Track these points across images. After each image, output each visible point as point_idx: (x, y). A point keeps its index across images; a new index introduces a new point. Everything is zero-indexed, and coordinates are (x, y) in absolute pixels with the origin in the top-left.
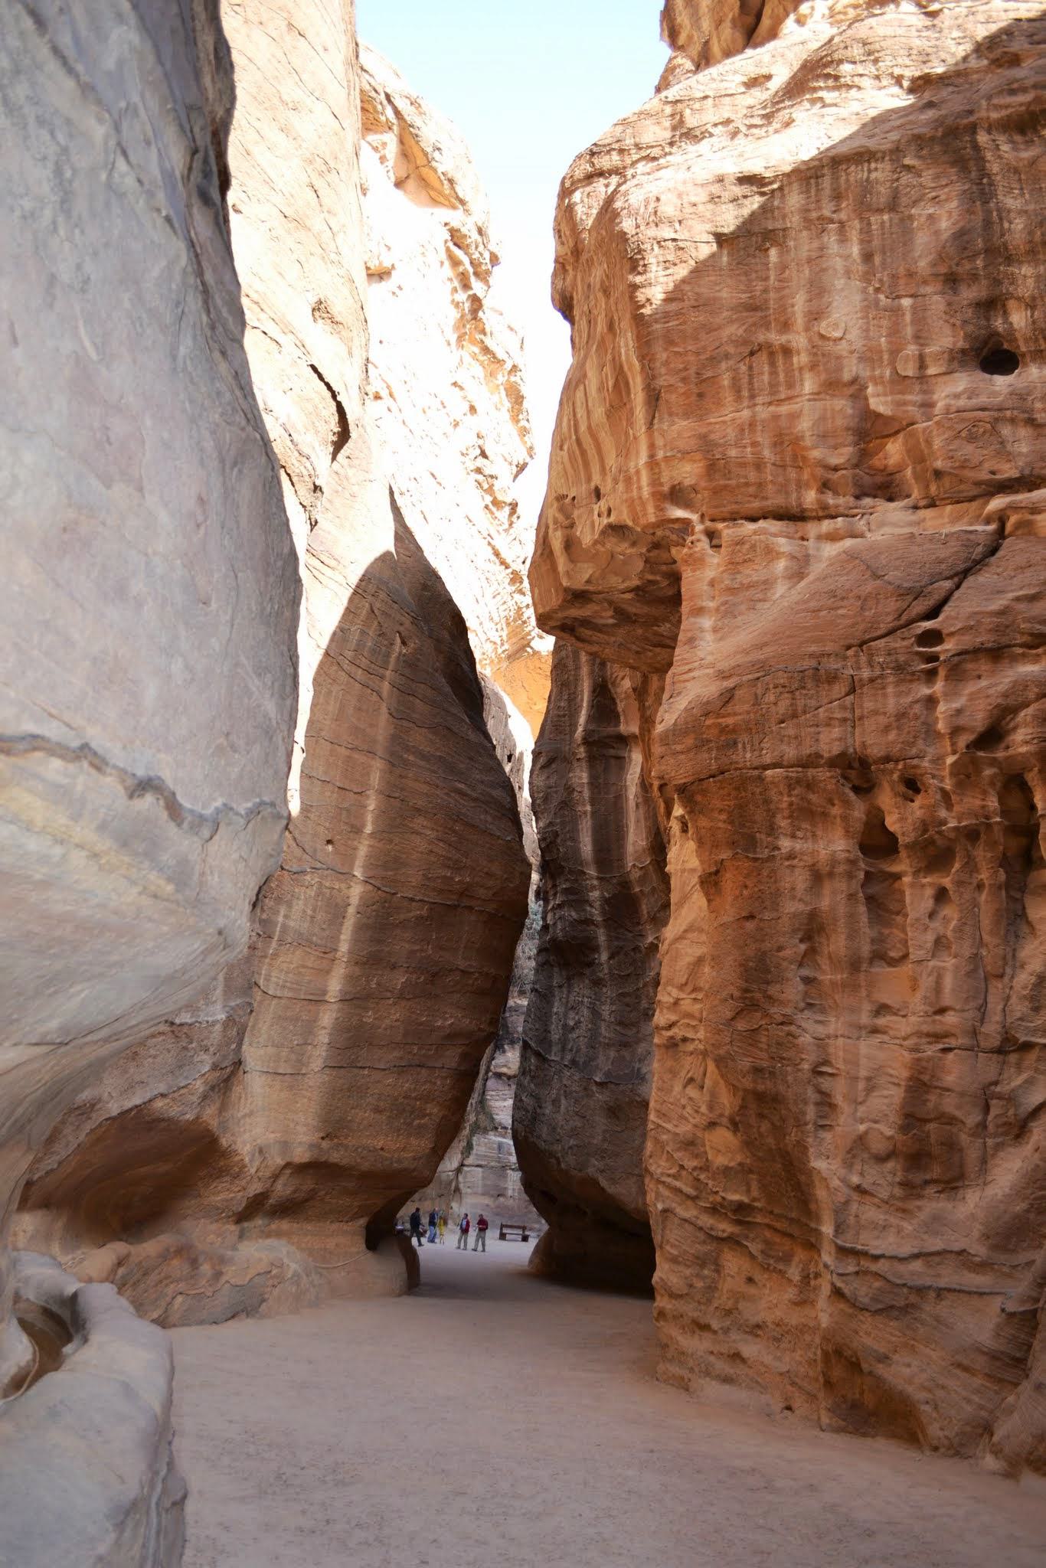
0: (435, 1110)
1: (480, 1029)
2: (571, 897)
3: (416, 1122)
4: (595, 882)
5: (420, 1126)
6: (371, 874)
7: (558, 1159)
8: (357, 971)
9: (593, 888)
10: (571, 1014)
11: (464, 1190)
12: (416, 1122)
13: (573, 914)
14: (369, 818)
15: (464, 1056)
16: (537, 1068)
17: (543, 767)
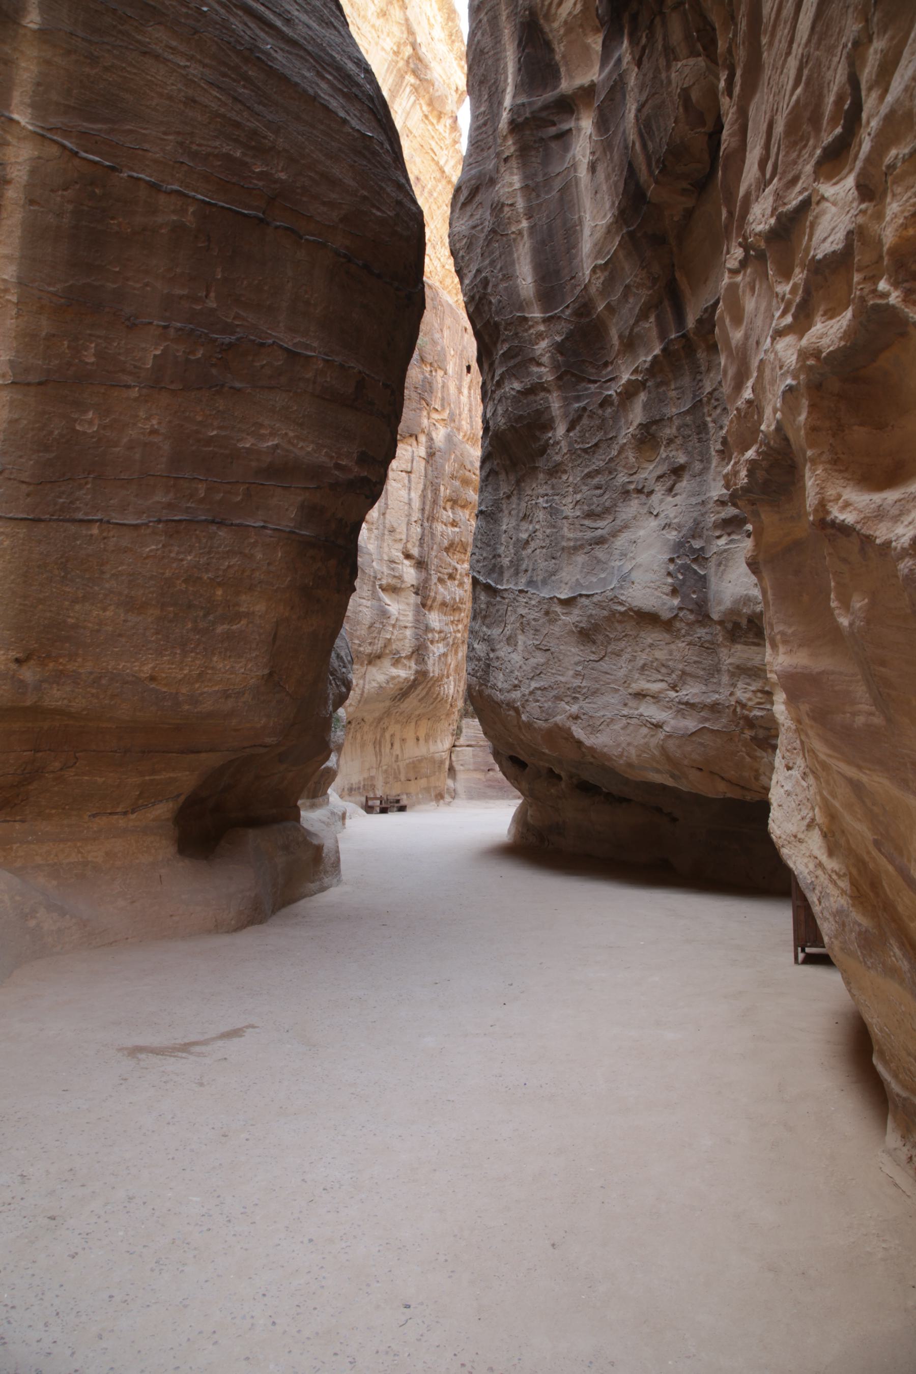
1: (338, 466)
2: (512, 363)
3: (220, 629)
4: (542, 328)
7: (516, 710)
8: (45, 325)
9: (540, 336)
10: (524, 525)
11: (457, 767)
12: (220, 629)
15: (311, 512)
16: (489, 604)
17: (464, 205)
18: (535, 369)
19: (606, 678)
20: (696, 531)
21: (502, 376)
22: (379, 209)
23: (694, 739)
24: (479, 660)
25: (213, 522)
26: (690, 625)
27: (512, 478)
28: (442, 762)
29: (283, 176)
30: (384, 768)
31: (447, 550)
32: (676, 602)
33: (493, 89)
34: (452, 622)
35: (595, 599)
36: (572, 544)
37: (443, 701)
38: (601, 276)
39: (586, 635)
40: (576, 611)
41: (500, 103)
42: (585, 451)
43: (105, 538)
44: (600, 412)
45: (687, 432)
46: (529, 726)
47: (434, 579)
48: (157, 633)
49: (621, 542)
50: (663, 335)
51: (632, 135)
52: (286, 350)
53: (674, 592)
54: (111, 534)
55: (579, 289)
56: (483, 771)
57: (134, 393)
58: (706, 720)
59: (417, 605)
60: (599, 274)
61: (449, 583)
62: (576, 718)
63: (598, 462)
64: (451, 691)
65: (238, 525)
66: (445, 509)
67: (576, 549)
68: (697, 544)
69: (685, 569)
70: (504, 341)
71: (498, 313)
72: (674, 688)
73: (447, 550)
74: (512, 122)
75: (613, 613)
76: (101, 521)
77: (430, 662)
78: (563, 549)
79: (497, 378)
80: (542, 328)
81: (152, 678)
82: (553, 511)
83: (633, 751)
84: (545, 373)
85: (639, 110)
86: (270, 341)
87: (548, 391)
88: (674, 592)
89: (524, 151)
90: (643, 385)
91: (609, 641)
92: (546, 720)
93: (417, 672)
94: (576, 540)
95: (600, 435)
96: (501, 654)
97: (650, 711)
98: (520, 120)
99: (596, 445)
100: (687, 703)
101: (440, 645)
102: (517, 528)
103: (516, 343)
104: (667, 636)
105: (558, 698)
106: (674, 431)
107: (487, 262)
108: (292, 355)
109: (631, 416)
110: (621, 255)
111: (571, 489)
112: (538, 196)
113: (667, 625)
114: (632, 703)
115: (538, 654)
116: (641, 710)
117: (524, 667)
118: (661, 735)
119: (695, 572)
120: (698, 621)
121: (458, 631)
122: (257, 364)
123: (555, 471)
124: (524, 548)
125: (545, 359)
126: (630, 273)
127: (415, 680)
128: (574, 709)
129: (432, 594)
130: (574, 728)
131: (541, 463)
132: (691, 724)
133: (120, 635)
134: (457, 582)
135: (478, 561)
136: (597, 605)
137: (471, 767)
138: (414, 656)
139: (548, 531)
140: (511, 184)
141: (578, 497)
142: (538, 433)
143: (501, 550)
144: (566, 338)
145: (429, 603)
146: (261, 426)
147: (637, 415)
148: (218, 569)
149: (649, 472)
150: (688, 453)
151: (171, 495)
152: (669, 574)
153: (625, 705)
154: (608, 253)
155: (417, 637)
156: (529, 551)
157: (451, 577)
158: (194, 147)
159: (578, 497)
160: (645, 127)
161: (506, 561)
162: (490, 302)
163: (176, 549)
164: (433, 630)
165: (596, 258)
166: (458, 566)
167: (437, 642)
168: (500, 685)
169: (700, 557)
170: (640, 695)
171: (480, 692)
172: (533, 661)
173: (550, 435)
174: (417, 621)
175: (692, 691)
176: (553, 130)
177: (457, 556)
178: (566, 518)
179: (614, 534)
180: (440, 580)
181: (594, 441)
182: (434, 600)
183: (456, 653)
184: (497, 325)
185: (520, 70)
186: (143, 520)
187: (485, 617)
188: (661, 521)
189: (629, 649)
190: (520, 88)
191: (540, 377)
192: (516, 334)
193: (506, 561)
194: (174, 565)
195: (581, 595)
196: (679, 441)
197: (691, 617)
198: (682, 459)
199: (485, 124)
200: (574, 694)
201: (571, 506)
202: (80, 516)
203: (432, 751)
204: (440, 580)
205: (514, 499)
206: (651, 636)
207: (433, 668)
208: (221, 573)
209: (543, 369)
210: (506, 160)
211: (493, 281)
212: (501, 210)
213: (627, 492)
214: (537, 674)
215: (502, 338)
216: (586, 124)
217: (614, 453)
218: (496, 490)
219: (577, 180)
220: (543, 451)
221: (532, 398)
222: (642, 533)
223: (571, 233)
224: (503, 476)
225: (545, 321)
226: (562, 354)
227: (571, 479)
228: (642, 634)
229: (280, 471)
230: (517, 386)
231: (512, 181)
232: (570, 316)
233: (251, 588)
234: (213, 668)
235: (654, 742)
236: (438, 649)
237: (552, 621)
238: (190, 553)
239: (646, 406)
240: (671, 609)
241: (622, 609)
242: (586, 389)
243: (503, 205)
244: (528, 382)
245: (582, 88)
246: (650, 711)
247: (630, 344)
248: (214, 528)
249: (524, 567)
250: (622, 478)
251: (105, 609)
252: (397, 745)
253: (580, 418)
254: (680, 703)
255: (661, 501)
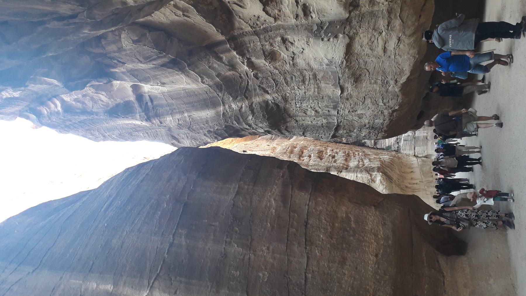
0: (344, 209)
1: (283, 176)
2: (241, 120)
3: (353, 225)
5: (357, 222)
6: (146, 282)
7: (393, 111)
9: (230, 107)
10: (309, 113)
12: (353, 225)
13: (250, 117)
14: (102, 287)
15: (302, 187)
16: (344, 129)
18: (243, 109)
19: (377, 69)
20: (309, 29)
21: (247, 124)
22: (181, 161)
23: (405, 20)
24: (370, 133)
25: (306, 226)
26: (351, 27)
27: (289, 119)
28: (423, 161)
29: (168, 196)
30: (426, 187)
31: (321, 159)
32: (341, 36)
33: (134, 130)
34: (354, 156)
35: (340, 75)
36: (316, 89)
37: (392, 160)
38: (206, 79)
39: (357, 79)
40: (346, 85)
41: (139, 126)
42: (277, 85)
43: (313, 271)
44: (260, 79)
45: (267, 37)
46: (401, 105)
47: (335, 164)
48: (355, 252)
49: (315, 66)
50: (228, 51)
51: (150, 65)
52: (236, 195)
53: (336, 37)
54: (311, 269)
55: (211, 90)
56: (427, 142)
57: (252, 256)
58: (395, 15)
59: (347, 172)
60: (204, 80)
61: (336, 158)
62: (396, 81)
63: (281, 79)
64: (387, 157)
65: (307, 215)
66: (303, 160)
67: (319, 88)
68: (315, 28)
69: (326, 33)
70: (233, 123)
71: (221, 126)
72: (381, 33)
73: (321, 159)
74: (146, 120)
75: (347, 66)
76: (305, 273)
77: (373, 166)
78: (318, 93)
79: (247, 127)
80: (227, 106)
81: (376, 256)
82: (303, 99)
83: (412, 51)
84: (245, 105)
85: (141, 62)
86: (232, 202)
87: (252, 103)
88: (336, 37)
89: (157, 115)
90: (249, 59)
91: (360, 67)
92: (398, 96)
93: (378, 172)
94: (315, 88)
95: (270, 79)
96: (367, 121)
97: (392, 45)
98: (146, 117)
99: (274, 80)
100: (388, 26)
101: (365, 161)
102: (310, 116)
103: (233, 118)
104: (357, 39)
105: (387, 91)
106: (267, 43)
107: (201, 131)
108: (238, 193)
109: (262, 65)
110: (197, 70)
111: (293, 91)
112: (175, 109)
113: (352, 39)
114: (388, 53)
115: (366, 103)
116: (392, 49)
117: (373, 109)
118: (403, 37)
119: (327, 27)
120: (350, 24)
121: (359, 154)
122: (241, 206)
123: (285, 99)
124: (319, 113)
125: (240, 105)
126: (204, 66)
127: (382, 172)
128: (392, 82)
129: (341, 165)
130: (401, 82)
131: (282, 105)
132: (397, 23)
133: (356, 268)
134: (336, 155)
135: (325, 135)
136: (343, 74)
137: (425, 147)
138: (371, 173)
139: (311, 101)
140: (170, 120)
141: (296, 88)
142: (270, 108)
143: (319, 123)
144: (231, 95)
145: (345, 166)
146: (266, 205)
147: (261, 62)
148: (326, 225)
149: (284, 55)
150: (276, 37)
151: (295, 243)
152: (329, 40)
153: (389, 57)
154: (196, 76)
155: (361, 171)
156: (320, 110)
157: (334, 157)
158: (156, 229)
159: (296, 88)
160: (148, 59)
161: (325, 121)
162: (217, 129)
163: (318, 242)
164: (358, 165)
165: (198, 82)
166: (329, 154)
167: (363, 163)
168: (381, 121)
169: (320, 26)
170: (385, 50)
171: (385, 132)
172: (370, 105)
173: (270, 102)
174: (354, 171)
175: (382, 23)
176: (150, 104)
177: (324, 154)
178: (305, 93)
179: (312, 69)
180: (335, 162)
181: (272, 81)
182: (344, 164)
183: (369, 155)
184: (226, 126)
185: (127, 117)
186: (305, 255)
187: (350, 131)
188: (305, 46)
189: (363, 57)
190: (134, 118)
191: (247, 107)
192: (230, 118)
193: (325, 121)
194: (325, 243)
195: (339, 83)
196: (271, 41)
197: (348, 27)
198: (279, 39)
199: (147, 133)
200: (385, 83)
201: (300, 91)
202: (303, 282)
203: (417, 166)
204: (335, 162)
205: (297, 119)
206: (357, 47)
207: (376, 164)
208: (328, 224)
209: (243, 106)
210: (161, 123)
211: (209, 129)
212: (180, 125)
213: (293, 64)
214: (375, 103)
215: (231, 124)
216: (146, 88)
217: (277, 72)
218: (294, 127)
219: (169, 92)
220: (277, 105)
221: (255, 110)
222: (311, 56)
223: (189, 94)
224: (288, 124)
225: (224, 105)
226: (237, 97)
227: (288, 92)
228: (356, 51)
229: (284, 198)
230: (250, 117)
231: (169, 120)
232: (222, 93)
233: (335, 212)
234: (371, 230)
235: (407, 41)
236: (367, 162)
237: (351, 97)
238: (319, 236)
239: (257, 58)
240: (344, 37)
241: (345, 62)
242: (251, 86)
243: (179, 124)
244: (249, 112)
245: (133, 91)
246: (392, 45)
247: (233, 66)
248: (309, 226)
249: (327, 112)
250: (287, 67)
251: (345, 274)
252: (415, 182)
253: (263, 88)
254: (388, 29)
255: (297, 47)
